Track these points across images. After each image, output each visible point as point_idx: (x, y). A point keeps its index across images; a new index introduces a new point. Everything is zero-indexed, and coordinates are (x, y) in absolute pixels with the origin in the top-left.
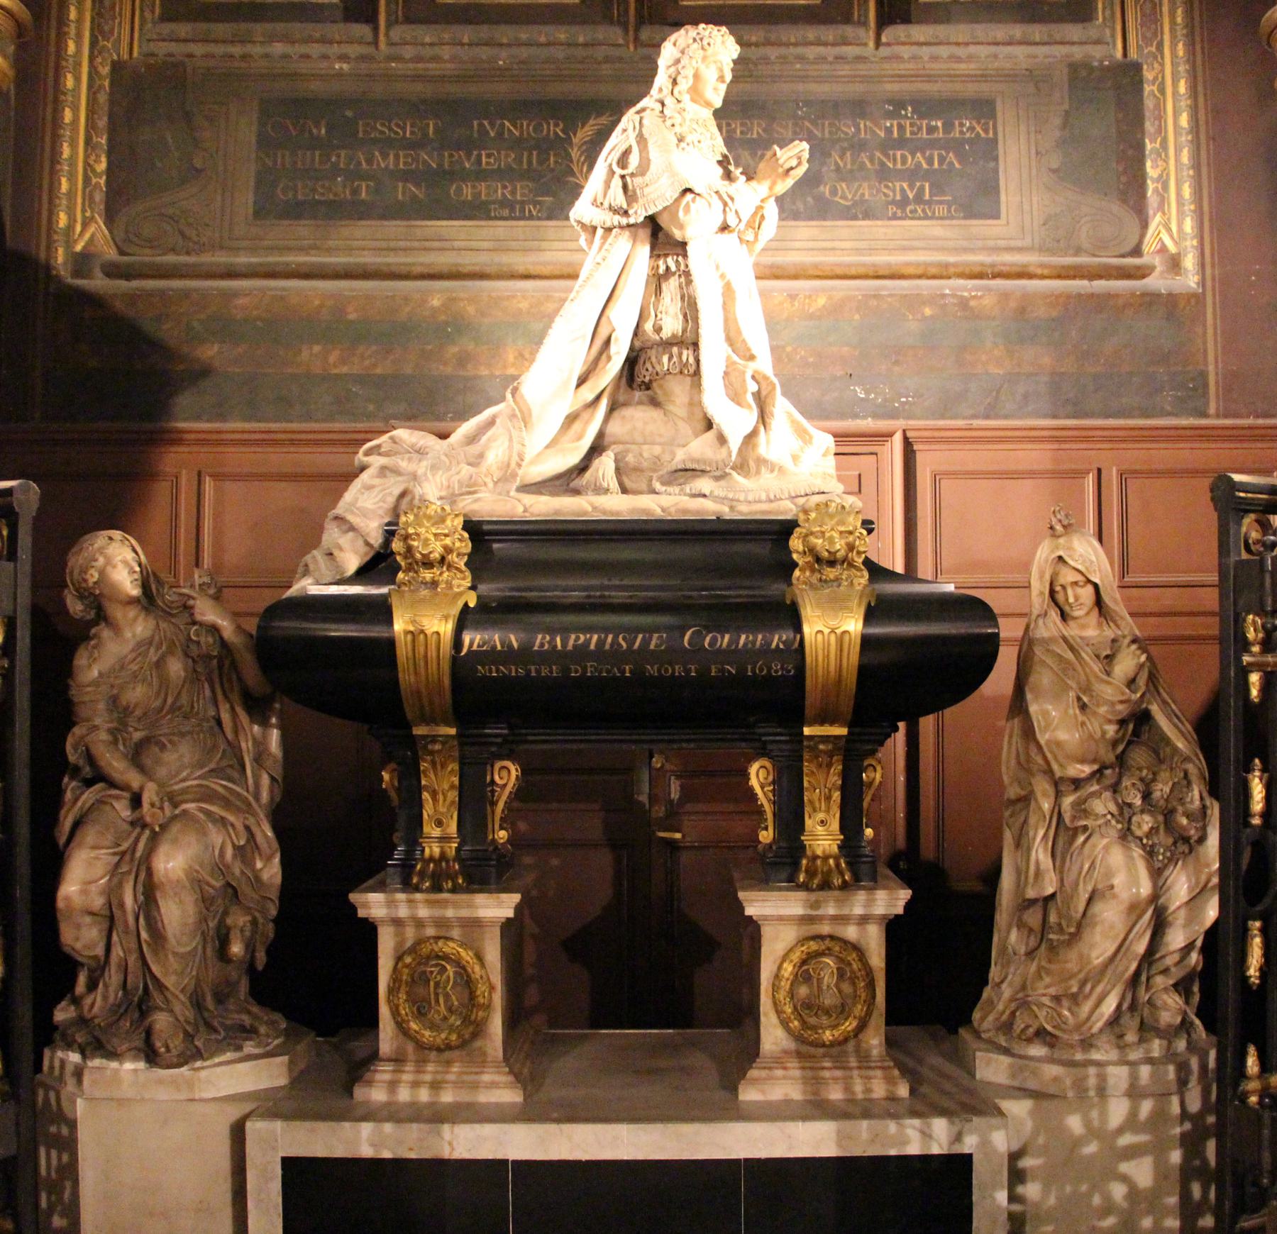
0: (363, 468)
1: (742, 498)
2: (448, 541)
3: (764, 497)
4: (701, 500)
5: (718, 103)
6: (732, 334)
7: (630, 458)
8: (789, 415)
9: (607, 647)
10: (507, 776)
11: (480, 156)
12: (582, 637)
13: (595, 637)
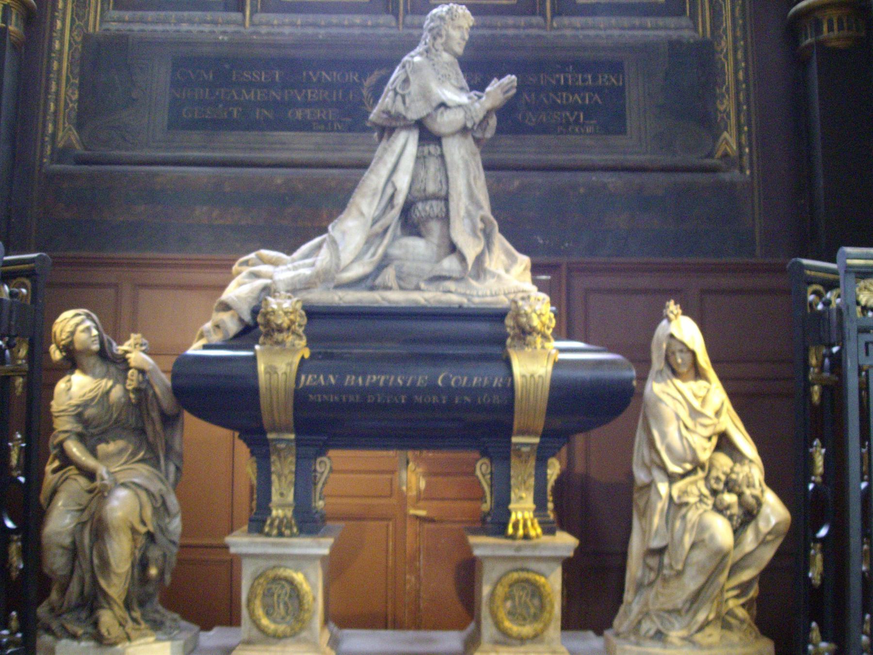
0: (239, 273)
1: (475, 293)
2: (292, 317)
3: (488, 293)
7: (405, 269)
11: (307, 93)
12: (375, 377)
13: (383, 378)
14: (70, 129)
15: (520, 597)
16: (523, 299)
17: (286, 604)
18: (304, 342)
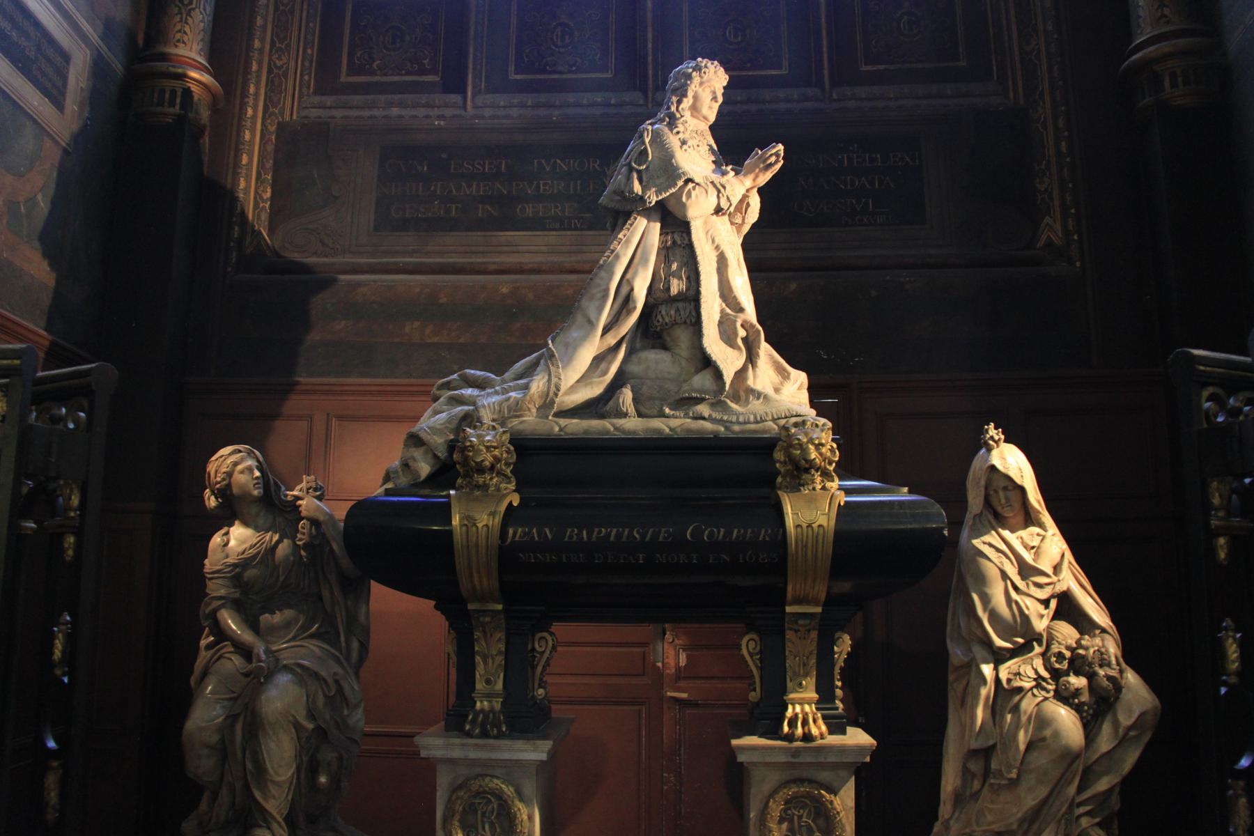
1: (734, 419)
2: (496, 452)
4: (702, 422)
5: (712, 118)
6: (726, 292)
8: (772, 357)
9: (624, 539)
13: (615, 531)
16: (796, 425)
17: (492, 824)
18: (512, 486)
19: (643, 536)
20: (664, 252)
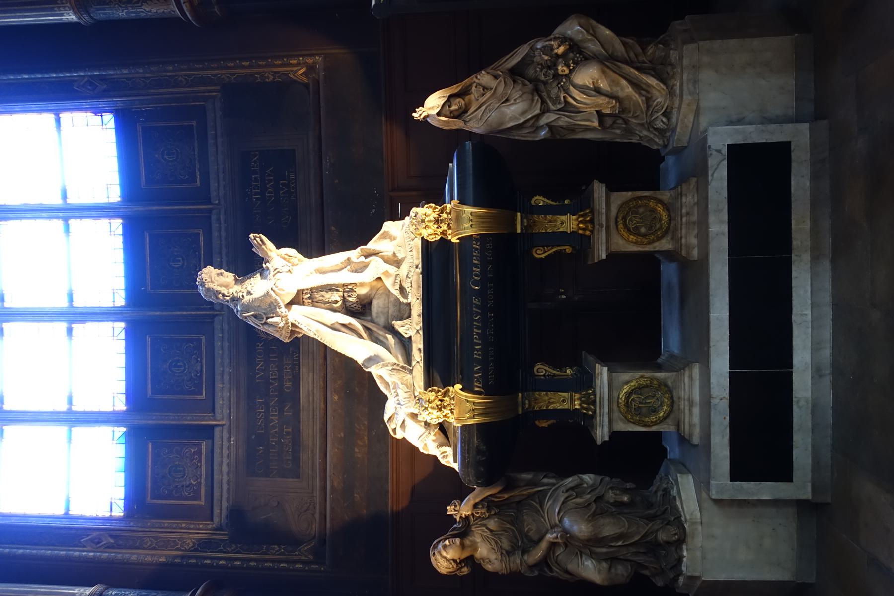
10: (542, 370)
14: (300, 550)
15: (638, 222)
18: (451, 389)
19: (478, 314)
20: (315, 304)
